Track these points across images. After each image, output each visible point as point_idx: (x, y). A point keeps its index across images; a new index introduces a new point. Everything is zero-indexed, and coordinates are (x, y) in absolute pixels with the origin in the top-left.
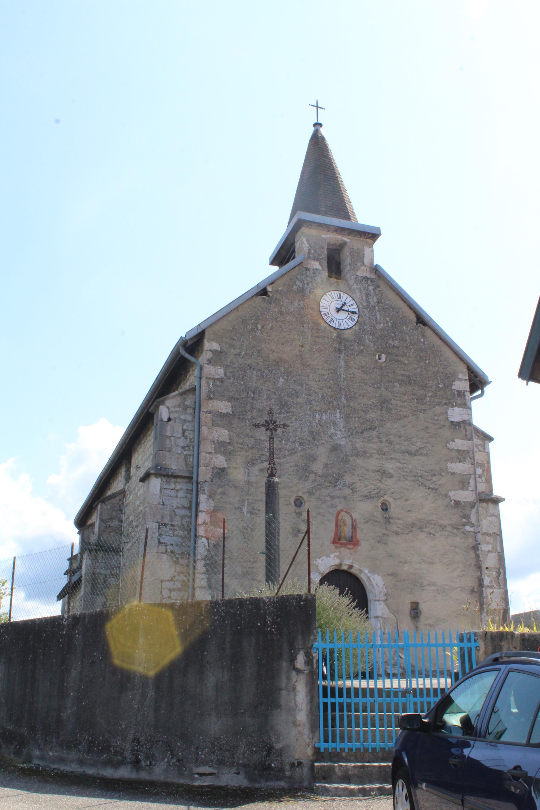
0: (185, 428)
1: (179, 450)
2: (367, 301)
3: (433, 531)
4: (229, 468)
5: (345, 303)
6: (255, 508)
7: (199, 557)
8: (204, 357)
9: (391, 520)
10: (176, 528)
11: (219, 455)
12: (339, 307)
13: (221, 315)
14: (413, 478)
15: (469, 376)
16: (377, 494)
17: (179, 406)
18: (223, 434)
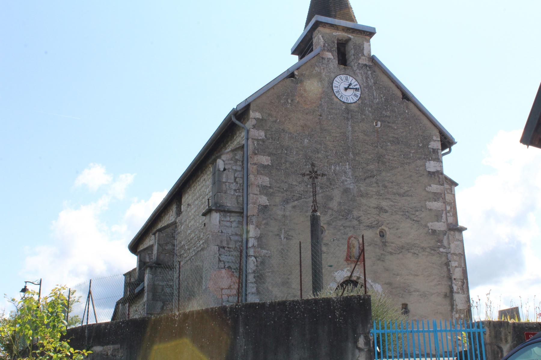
0: (236, 176)
1: (232, 192)
2: (367, 82)
3: (417, 252)
4: (270, 205)
5: (351, 84)
6: (289, 234)
7: (250, 271)
8: (249, 124)
9: (387, 244)
10: (232, 250)
11: (263, 196)
12: (346, 86)
13: (262, 92)
14: (402, 213)
15: (441, 138)
16: (377, 224)
17: (232, 160)
18: (265, 180)
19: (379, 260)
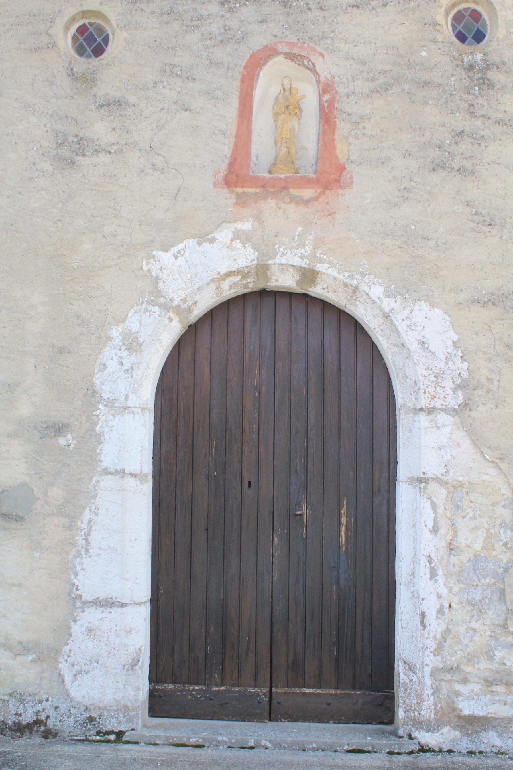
9: (492, 75)
19: (437, 167)
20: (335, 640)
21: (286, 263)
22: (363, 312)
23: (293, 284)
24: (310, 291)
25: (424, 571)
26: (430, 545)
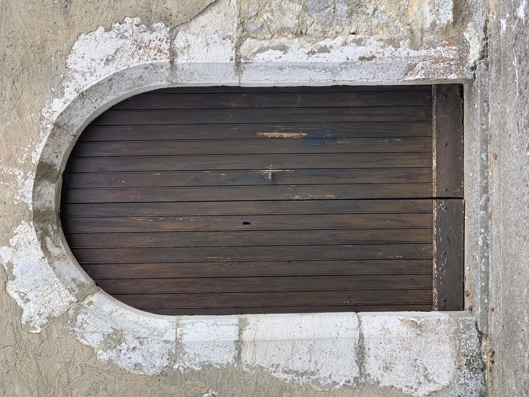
20: (387, 141)
21: (31, 193)
22: (79, 118)
23: (53, 186)
24: (60, 170)
25: (321, 58)
26: (297, 52)
